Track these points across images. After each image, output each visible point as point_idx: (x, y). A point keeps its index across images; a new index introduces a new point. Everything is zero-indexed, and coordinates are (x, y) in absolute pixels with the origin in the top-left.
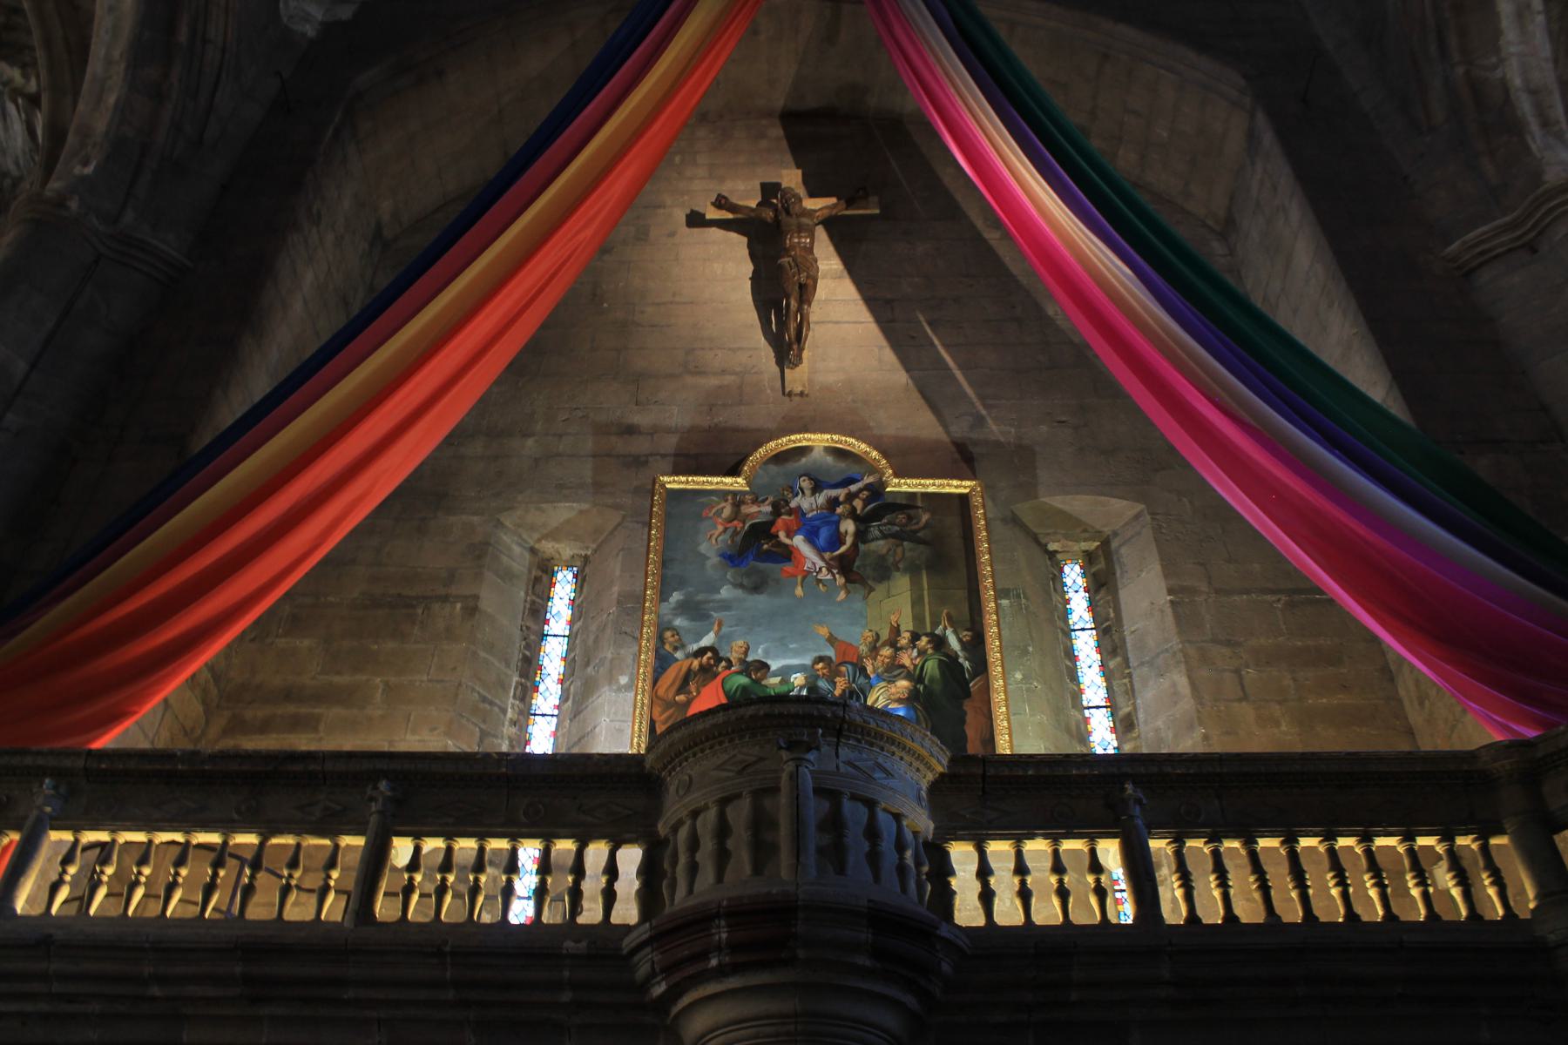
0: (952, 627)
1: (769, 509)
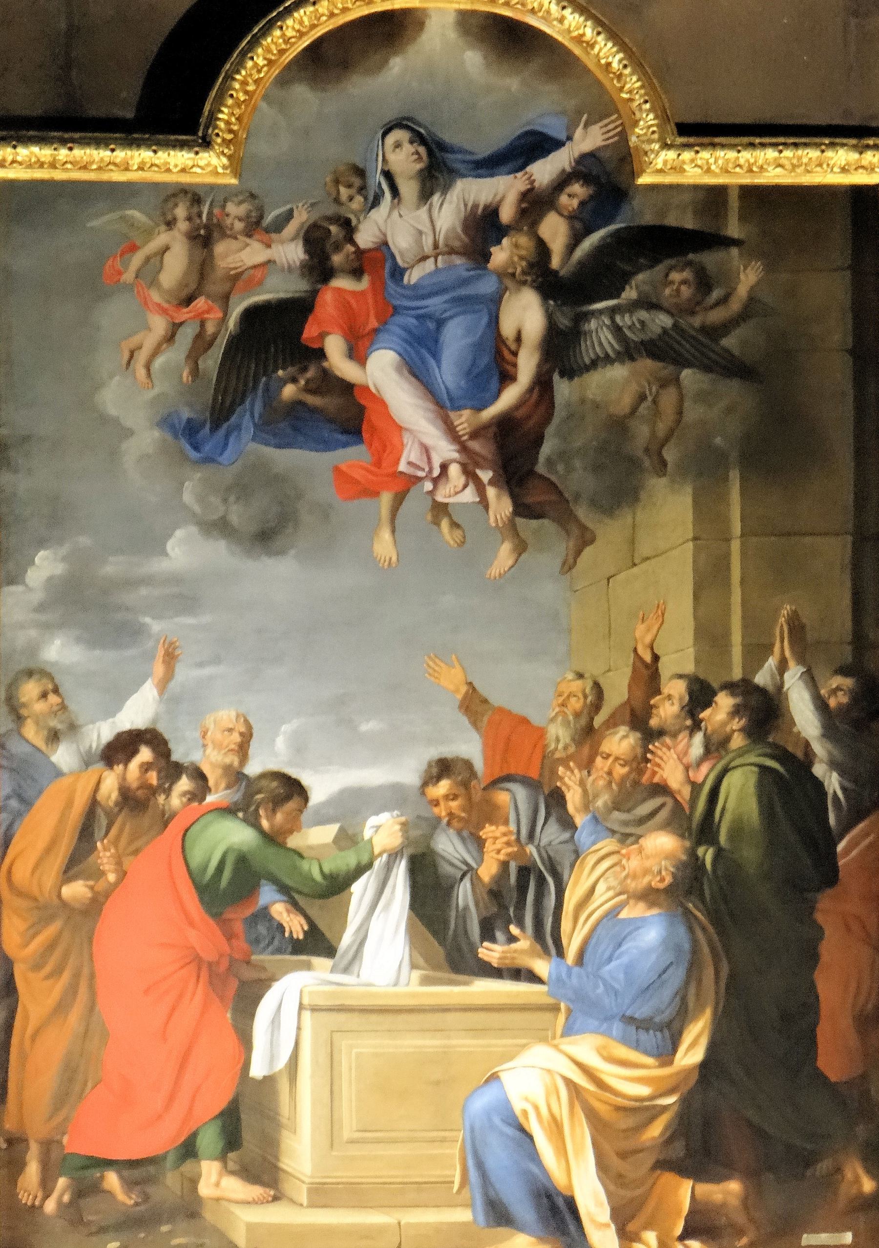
0: (801, 659)
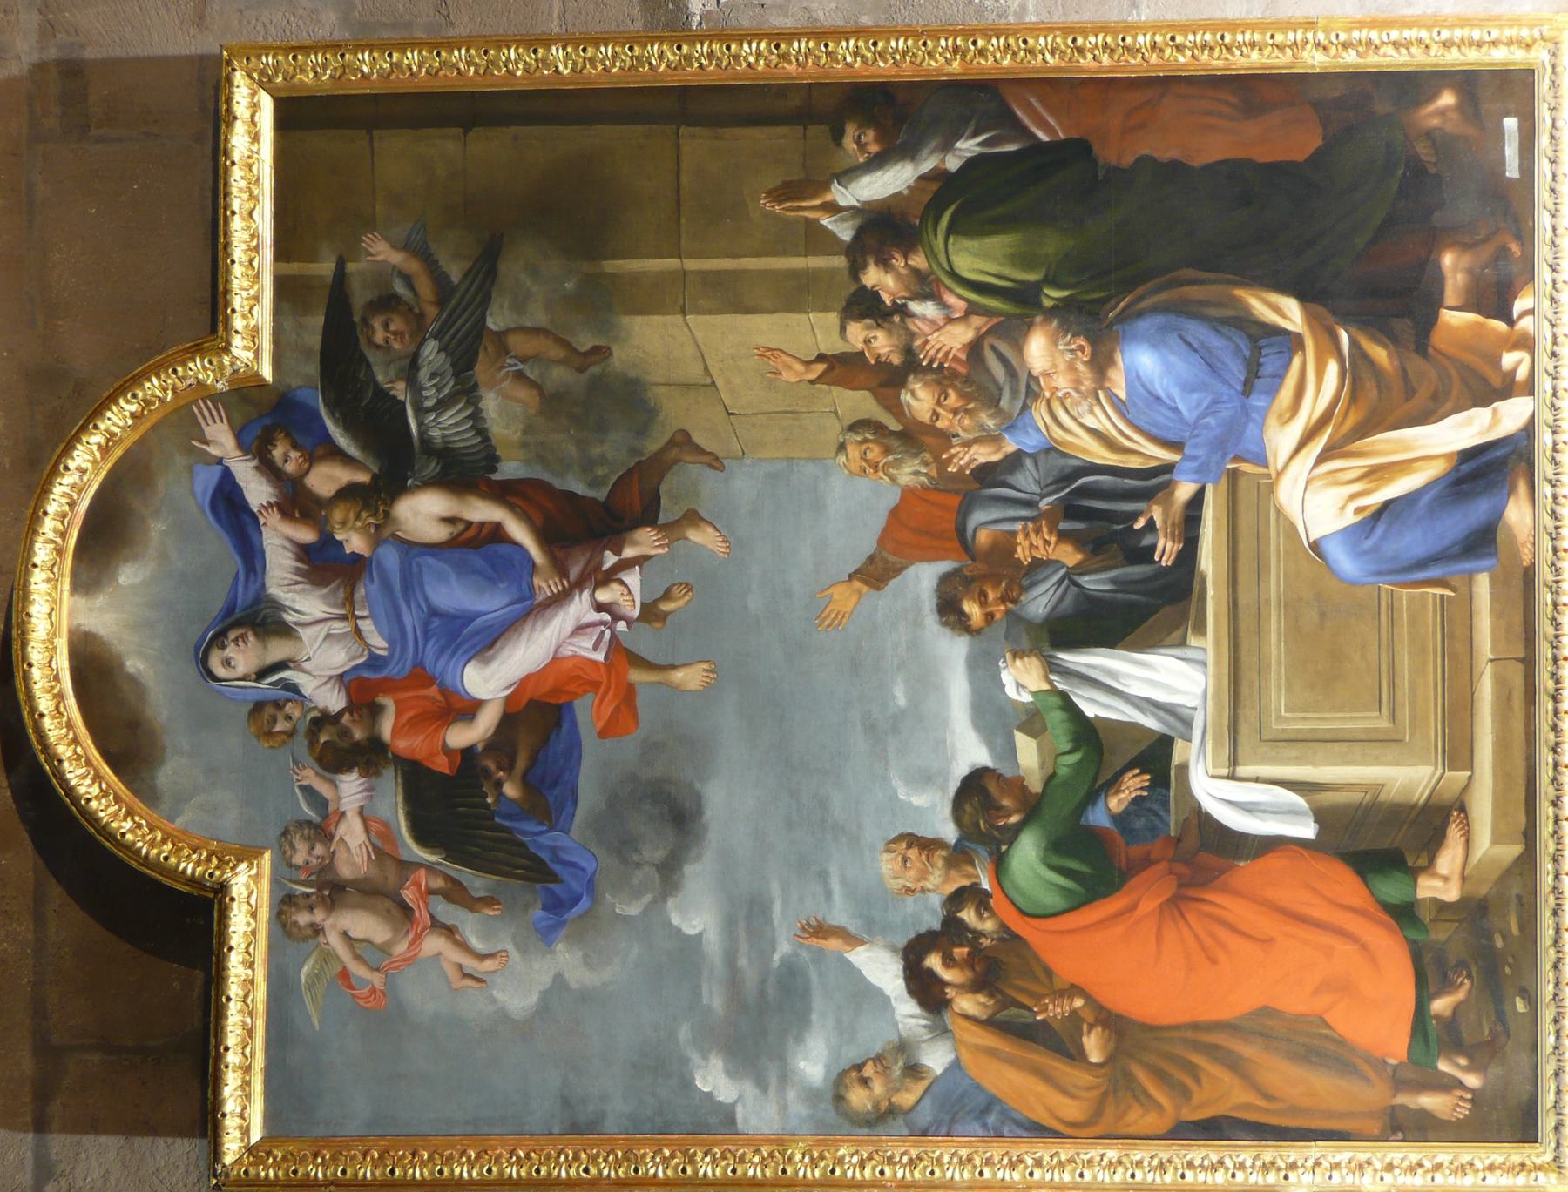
0: (826, 187)
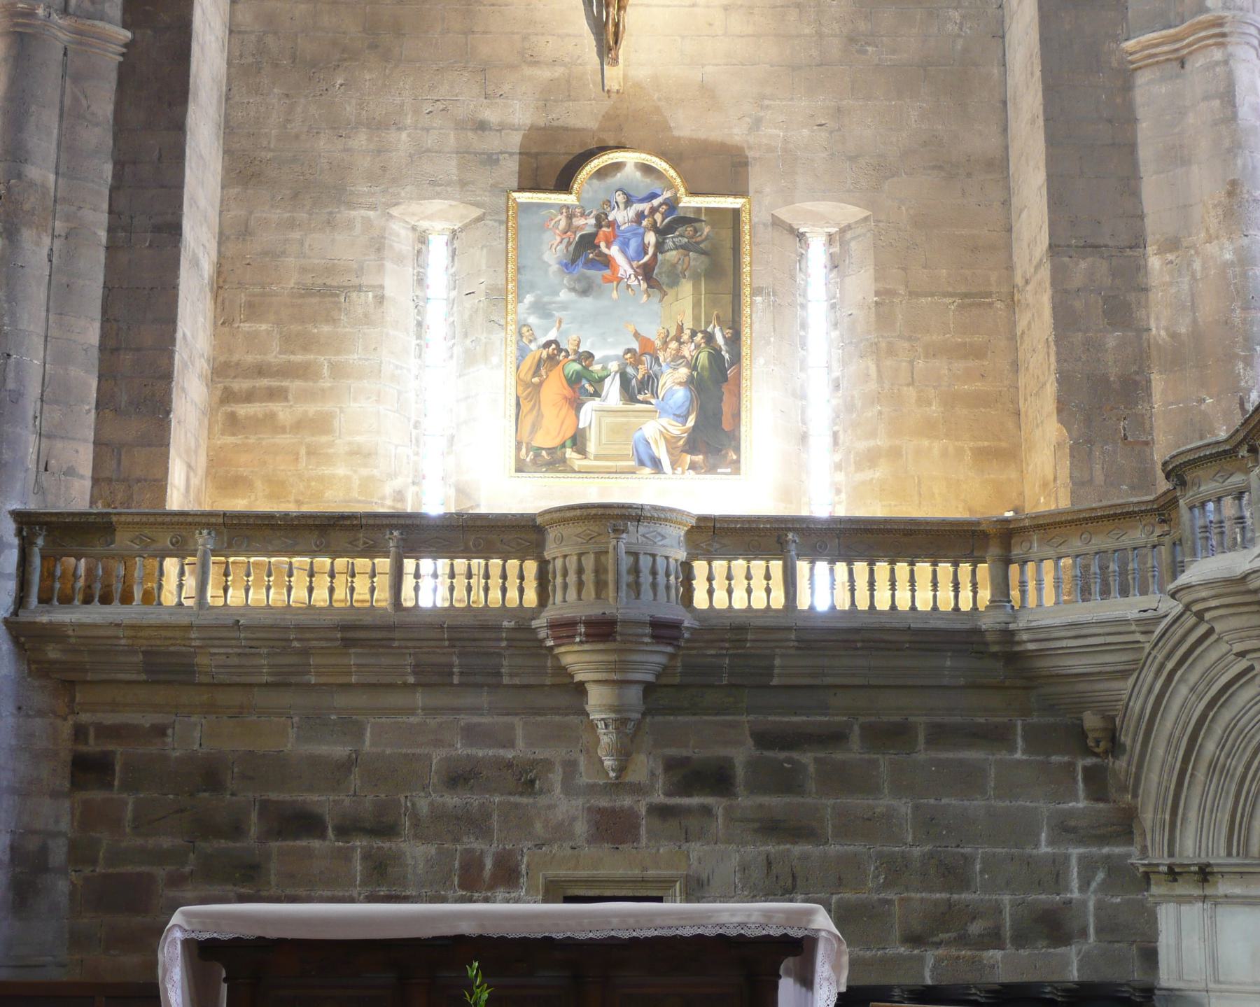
0: (719, 325)
1: (592, 221)
